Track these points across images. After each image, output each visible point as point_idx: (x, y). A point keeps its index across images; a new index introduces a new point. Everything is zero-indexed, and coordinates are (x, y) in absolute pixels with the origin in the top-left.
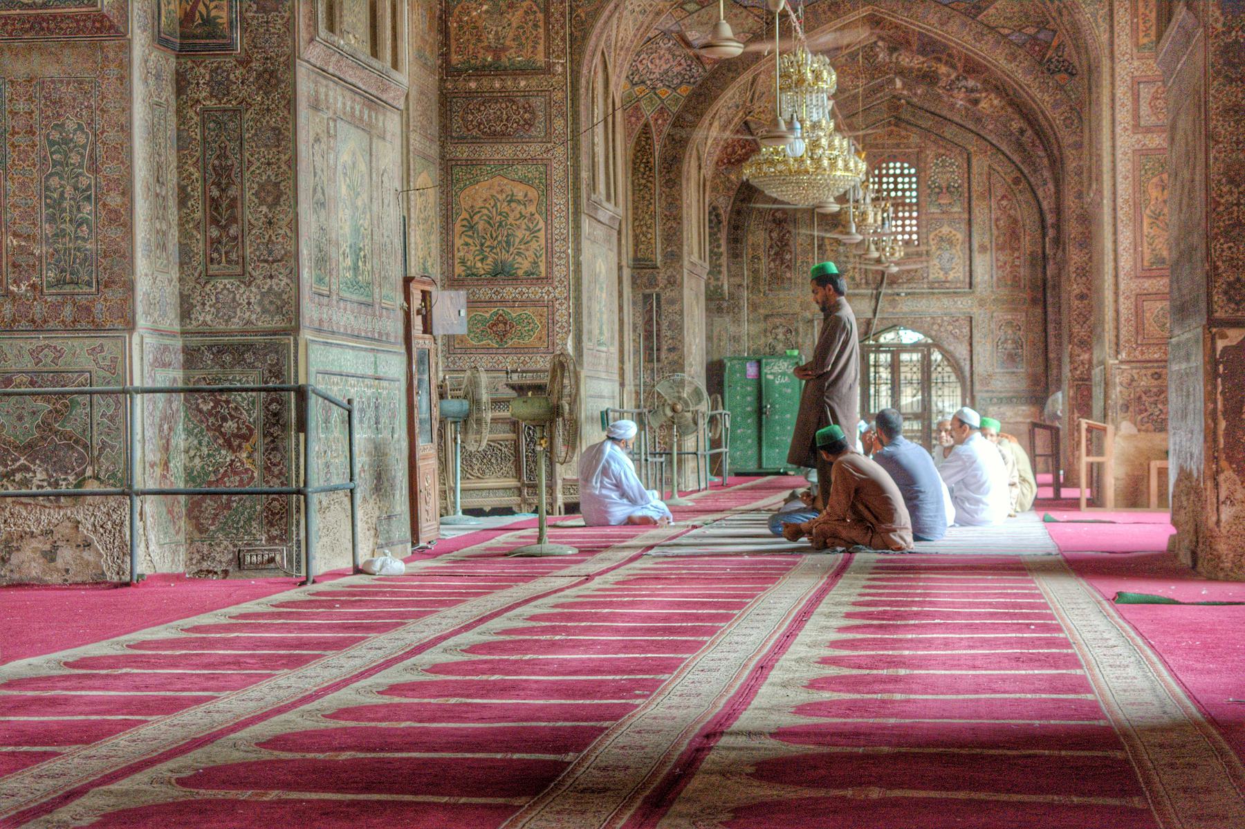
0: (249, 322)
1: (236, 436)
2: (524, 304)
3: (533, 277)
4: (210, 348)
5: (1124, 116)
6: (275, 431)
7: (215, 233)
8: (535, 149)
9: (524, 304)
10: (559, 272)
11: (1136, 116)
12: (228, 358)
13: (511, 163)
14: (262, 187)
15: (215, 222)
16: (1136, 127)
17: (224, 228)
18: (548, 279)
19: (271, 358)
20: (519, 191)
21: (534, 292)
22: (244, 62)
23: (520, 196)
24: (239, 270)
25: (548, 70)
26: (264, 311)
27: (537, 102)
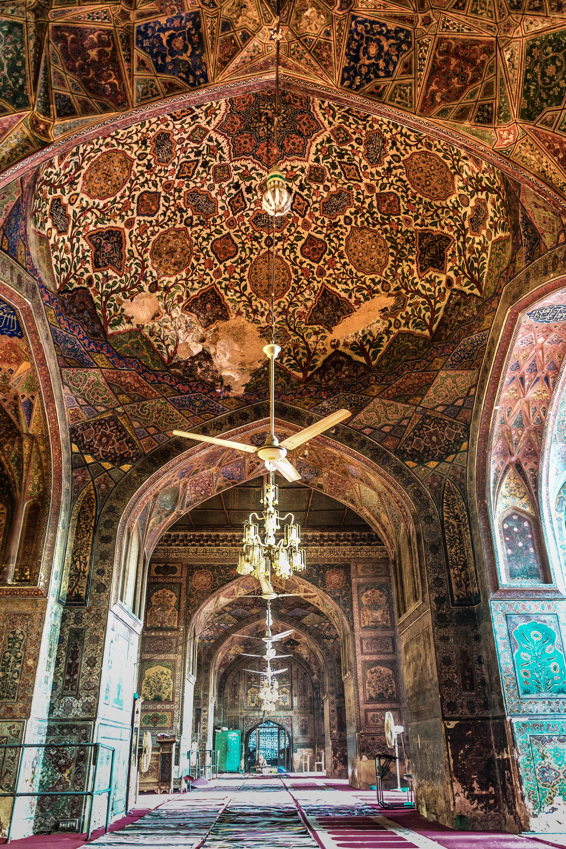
0: (77, 715)
1: (63, 766)
2: (164, 711)
3: (168, 701)
4: (59, 726)
5: (358, 650)
6: (81, 764)
7: (68, 677)
8: (172, 656)
9: (164, 711)
10: (177, 699)
11: (362, 649)
12: (65, 731)
13: (163, 660)
14: (89, 659)
15: (69, 673)
16: (362, 653)
17: (73, 676)
18: (172, 702)
19: (84, 731)
20: (165, 670)
21: (168, 707)
22: (89, 611)
23: (165, 672)
24: (75, 693)
25: (178, 629)
26: (83, 710)
27: (174, 640)
